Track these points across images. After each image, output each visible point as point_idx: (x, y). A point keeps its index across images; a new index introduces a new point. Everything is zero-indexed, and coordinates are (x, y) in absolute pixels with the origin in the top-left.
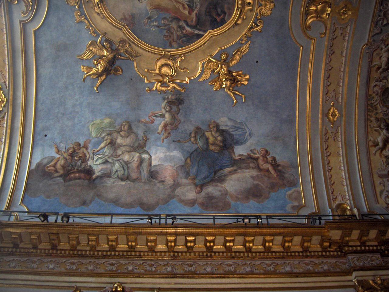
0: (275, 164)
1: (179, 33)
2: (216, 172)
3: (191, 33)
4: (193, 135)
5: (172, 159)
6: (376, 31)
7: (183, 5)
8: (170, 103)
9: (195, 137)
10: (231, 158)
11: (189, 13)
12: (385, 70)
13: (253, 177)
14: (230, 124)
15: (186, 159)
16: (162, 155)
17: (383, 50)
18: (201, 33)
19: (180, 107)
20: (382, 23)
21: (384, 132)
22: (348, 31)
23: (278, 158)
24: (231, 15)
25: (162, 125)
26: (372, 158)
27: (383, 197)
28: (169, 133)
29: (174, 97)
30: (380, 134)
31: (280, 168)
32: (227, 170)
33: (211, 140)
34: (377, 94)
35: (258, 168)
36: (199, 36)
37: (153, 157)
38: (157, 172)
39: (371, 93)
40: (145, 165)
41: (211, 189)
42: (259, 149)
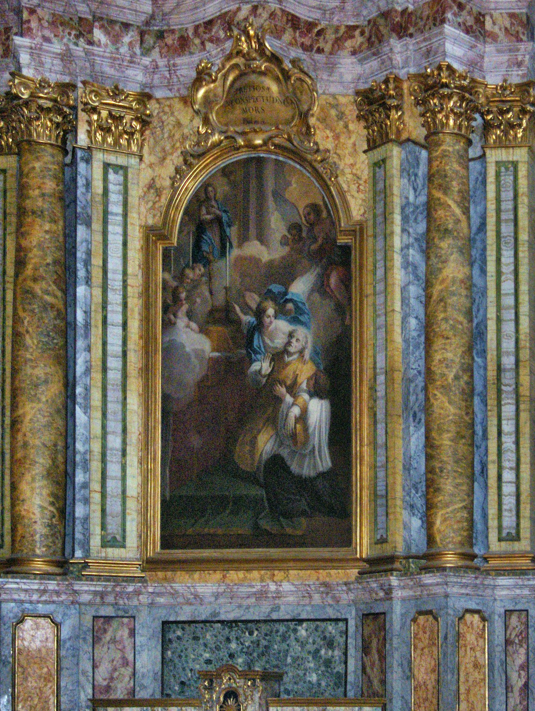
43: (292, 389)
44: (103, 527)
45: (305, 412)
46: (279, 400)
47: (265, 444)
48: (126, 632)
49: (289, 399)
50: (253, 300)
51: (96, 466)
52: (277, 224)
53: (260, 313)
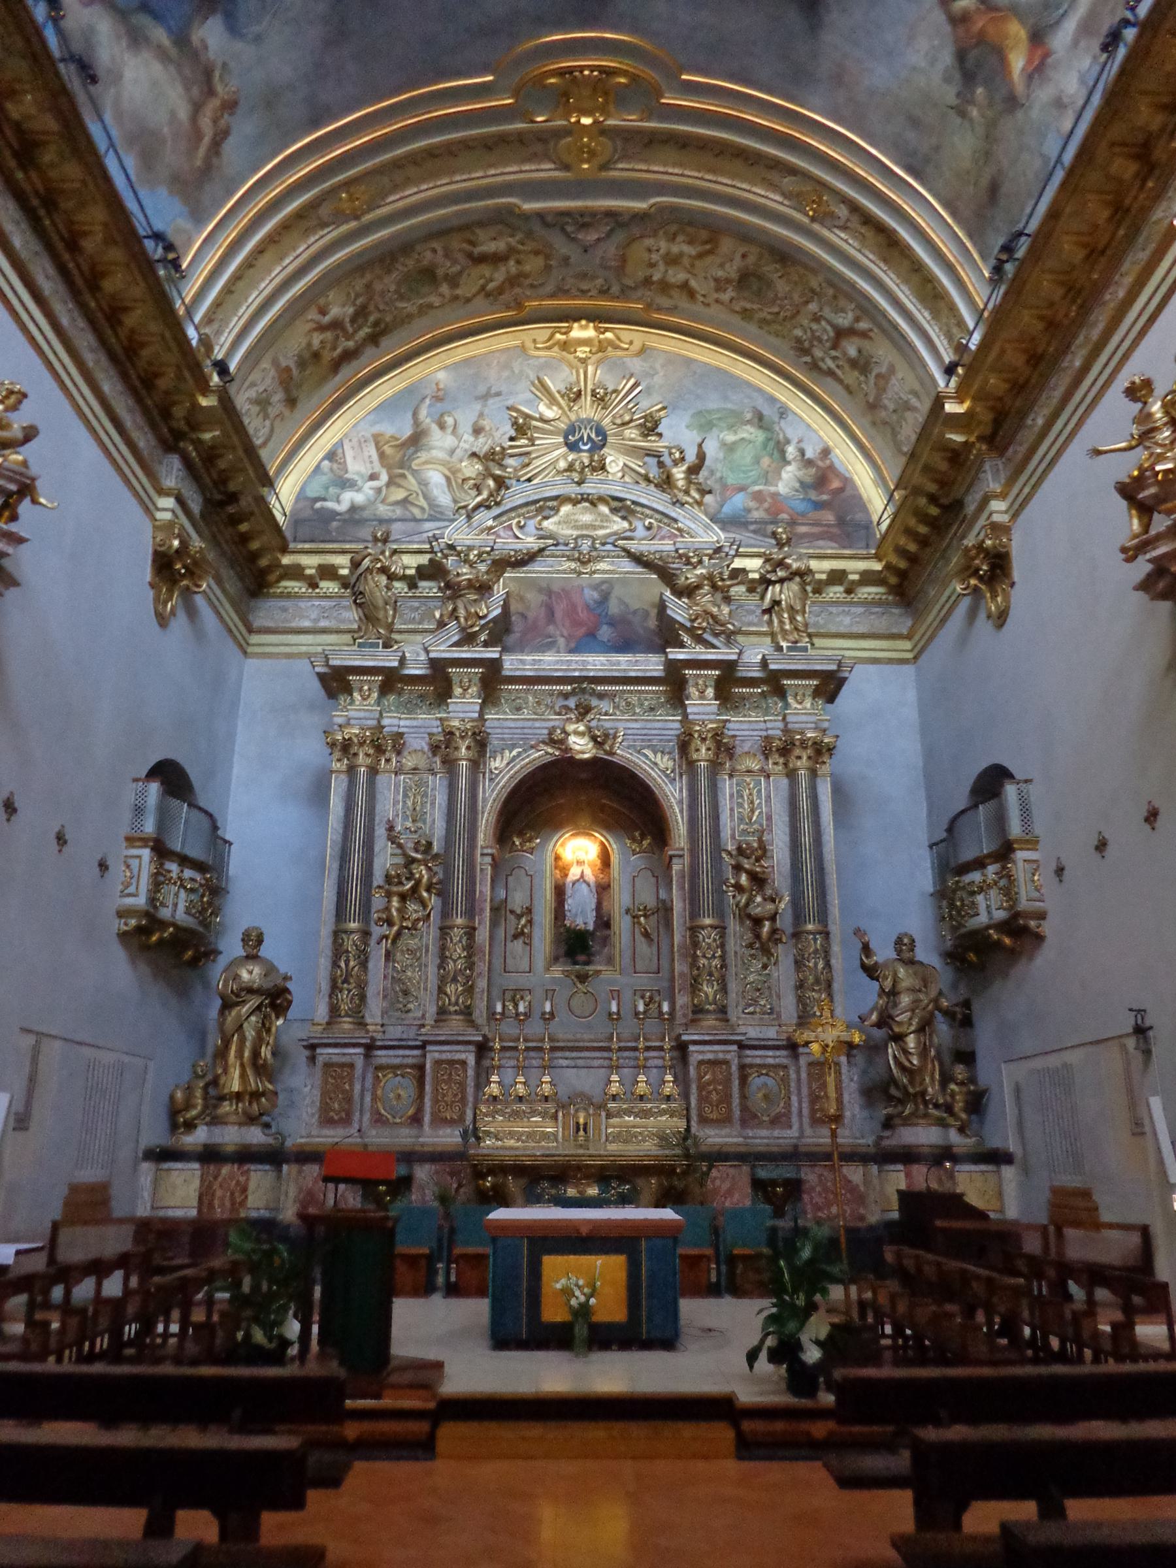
6: (549, 219)
12: (470, 256)
13: (173, 114)
17: (510, 239)
20: (567, 223)
21: (351, 310)
22: (543, 166)
26: (297, 322)
27: (247, 395)
30: (344, 306)
31: (215, 161)
32: (160, 35)
34: (418, 261)
35: (197, 108)
39: (418, 248)
42: (234, 84)
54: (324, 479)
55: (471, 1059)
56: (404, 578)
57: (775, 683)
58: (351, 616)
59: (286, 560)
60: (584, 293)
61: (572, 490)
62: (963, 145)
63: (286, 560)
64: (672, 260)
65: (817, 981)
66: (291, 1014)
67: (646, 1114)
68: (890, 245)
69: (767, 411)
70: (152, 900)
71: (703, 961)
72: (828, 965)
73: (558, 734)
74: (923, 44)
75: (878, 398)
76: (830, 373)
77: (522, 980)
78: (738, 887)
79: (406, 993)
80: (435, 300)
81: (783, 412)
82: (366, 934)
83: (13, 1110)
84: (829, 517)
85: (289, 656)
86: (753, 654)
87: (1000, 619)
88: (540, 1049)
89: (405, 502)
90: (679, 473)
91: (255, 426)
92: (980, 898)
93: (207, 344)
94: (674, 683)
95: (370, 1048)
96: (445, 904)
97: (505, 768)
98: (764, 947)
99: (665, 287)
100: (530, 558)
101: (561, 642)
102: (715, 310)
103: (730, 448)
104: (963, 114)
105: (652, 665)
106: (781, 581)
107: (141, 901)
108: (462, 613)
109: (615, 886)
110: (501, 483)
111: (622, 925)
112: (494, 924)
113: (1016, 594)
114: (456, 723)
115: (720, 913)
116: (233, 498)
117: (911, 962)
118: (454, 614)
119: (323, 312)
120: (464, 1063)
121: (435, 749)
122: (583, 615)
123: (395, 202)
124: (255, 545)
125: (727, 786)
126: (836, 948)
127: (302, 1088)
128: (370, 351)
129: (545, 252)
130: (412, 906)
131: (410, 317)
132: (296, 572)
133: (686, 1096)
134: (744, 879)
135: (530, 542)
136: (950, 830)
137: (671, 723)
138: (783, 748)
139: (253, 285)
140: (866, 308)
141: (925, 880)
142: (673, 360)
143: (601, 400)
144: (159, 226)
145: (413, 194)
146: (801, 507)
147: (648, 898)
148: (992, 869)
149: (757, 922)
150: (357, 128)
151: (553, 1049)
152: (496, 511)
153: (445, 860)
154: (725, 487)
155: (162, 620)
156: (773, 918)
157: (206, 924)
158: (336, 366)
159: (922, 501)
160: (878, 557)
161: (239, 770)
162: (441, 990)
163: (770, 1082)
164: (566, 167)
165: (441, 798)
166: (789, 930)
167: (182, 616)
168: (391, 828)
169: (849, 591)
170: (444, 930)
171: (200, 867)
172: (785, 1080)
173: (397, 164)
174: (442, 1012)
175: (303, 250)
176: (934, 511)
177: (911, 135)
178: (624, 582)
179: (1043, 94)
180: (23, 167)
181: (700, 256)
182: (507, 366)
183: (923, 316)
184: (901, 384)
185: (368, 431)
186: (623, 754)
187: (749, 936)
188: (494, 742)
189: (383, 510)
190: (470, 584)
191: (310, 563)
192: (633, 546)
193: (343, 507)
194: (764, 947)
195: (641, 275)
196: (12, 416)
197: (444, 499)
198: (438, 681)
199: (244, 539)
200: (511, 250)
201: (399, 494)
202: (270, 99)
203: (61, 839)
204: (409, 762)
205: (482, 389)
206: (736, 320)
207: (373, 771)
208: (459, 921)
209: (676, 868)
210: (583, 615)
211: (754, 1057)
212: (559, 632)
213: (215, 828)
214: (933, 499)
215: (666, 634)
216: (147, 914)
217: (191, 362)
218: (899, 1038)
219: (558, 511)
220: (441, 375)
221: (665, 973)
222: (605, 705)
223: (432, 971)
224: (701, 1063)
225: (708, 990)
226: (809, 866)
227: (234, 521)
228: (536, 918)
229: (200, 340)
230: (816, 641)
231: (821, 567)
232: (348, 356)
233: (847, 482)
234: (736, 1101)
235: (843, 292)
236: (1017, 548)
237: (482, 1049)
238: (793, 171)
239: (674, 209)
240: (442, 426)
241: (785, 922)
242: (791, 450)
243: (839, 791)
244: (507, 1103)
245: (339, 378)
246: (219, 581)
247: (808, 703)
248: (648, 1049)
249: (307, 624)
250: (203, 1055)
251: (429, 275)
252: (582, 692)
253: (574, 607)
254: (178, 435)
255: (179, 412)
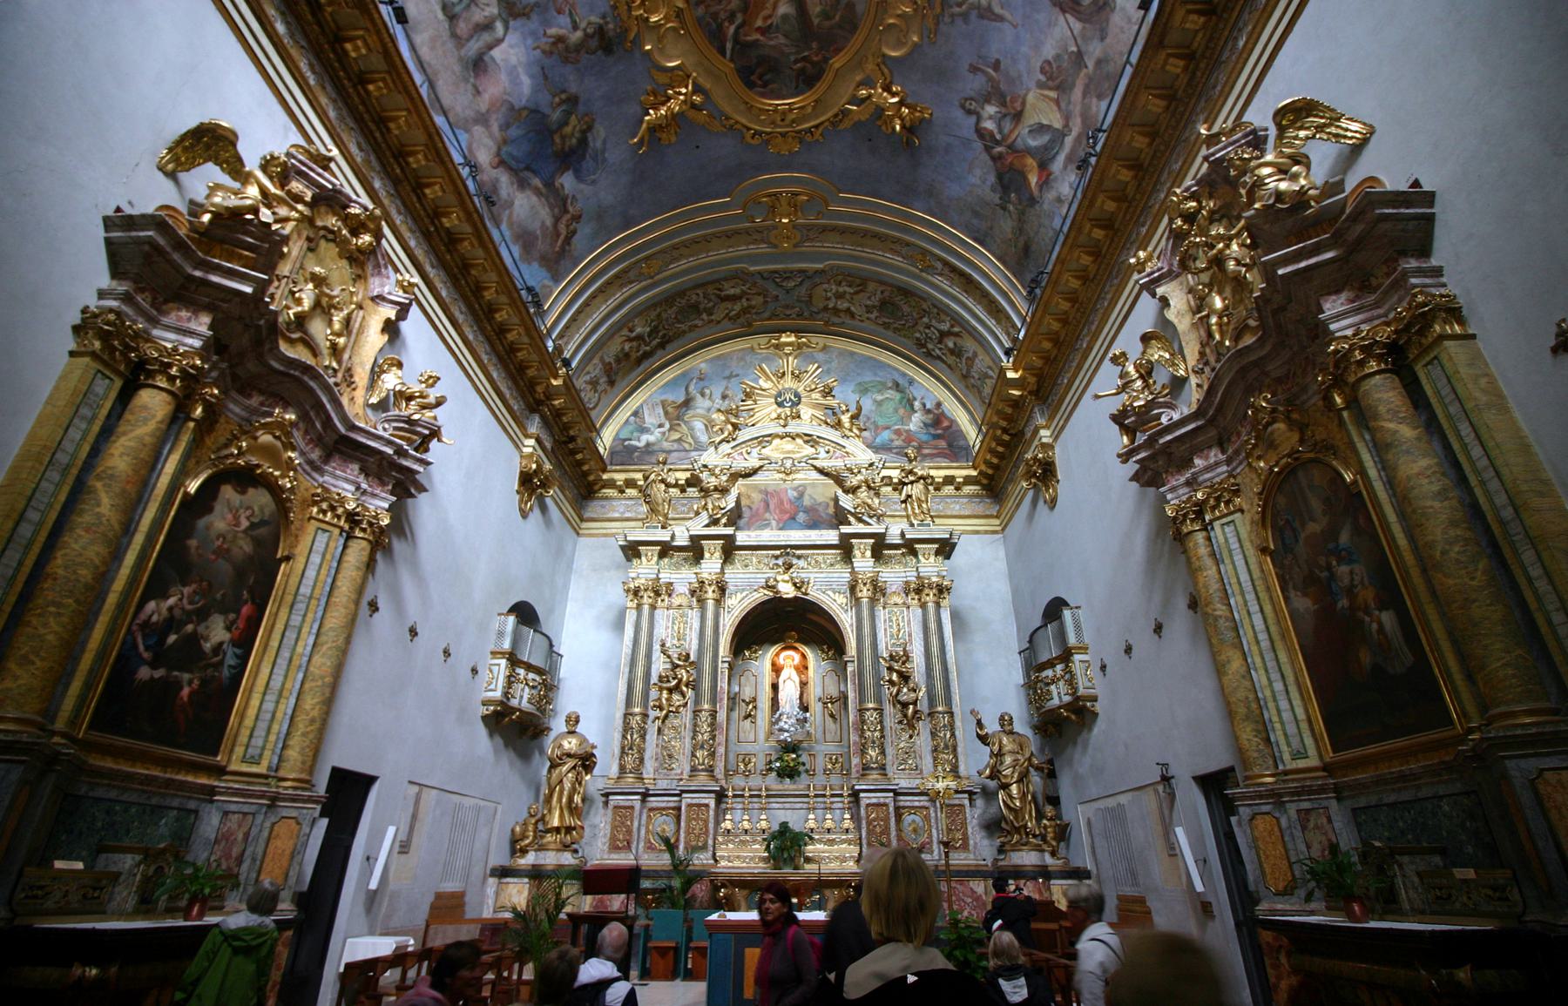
0: (568, 240)
1: (723, 15)
2: (528, 168)
3: (725, 36)
4: (563, 96)
5: (515, 80)
7: (770, 16)
8: (600, 30)
9: (562, 102)
10: (553, 177)
11: (759, 29)
12: (719, 296)
14: (599, 144)
15: (525, 108)
16: (514, 60)
18: (728, 53)
19: (599, 52)
23: (576, 237)
24: (764, 95)
25: (562, 32)
28: (551, 53)
29: (611, 34)
32: (537, 182)
33: (568, 130)
35: (557, 220)
36: (722, 52)
37: (504, 45)
38: (485, 71)
40: (486, 37)
41: (504, 180)
42: (579, 205)
43: (1367, 612)
44: (1289, 745)
45: (1380, 624)
46: (1363, 621)
47: (1365, 658)
48: (1325, 820)
49: (1367, 619)
50: (1322, 561)
51: (1271, 705)
52: (1316, 505)
53: (1329, 567)
54: (631, 428)
55: (712, 803)
56: (676, 485)
57: (910, 547)
58: (645, 508)
59: (605, 477)
60: (788, 317)
61: (780, 430)
62: (1006, 225)
63: (605, 477)
64: (839, 296)
65: (946, 747)
66: (596, 771)
67: (831, 842)
68: (969, 284)
69: (901, 381)
70: (506, 694)
71: (868, 734)
72: (953, 735)
73: (771, 583)
74: (978, 172)
75: (968, 371)
76: (939, 358)
77: (749, 748)
78: (891, 682)
79: (670, 756)
80: (700, 323)
81: (911, 382)
82: (645, 716)
83: (399, 838)
84: (943, 444)
85: (605, 535)
86: (895, 530)
87: (1052, 503)
88: (759, 796)
89: (680, 440)
90: (845, 419)
91: (588, 396)
92: (1053, 687)
93: (559, 349)
94: (845, 548)
95: (645, 795)
96: (697, 695)
97: (738, 605)
98: (910, 723)
99: (836, 311)
100: (755, 471)
101: (774, 523)
102: (866, 324)
103: (879, 404)
104: (1004, 208)
105: (831, 536)
106: (912, 483)
107: (498, 694)
108: (710, 506)
109: (811, 683)
110: (736, 427)
111: (816, 708)
112: (731, 709)
113: (1059, 487)
114: (705, 575)
115: (879, 700)
116: (572, 439)
117: (1011, 733)
118: (705, 507)
119: (631, 331)
120: (707, 806)
121: (693, 593)
122: (787, 506)
123: (675, 268)
124: (585, 468)
125: (881, 614)
126: (958, 723)
127: (599, 823)
128: (660, 352)
129: (764, 293)
130: (676, 697)
131: (684, 332)
132: (611, 484)
133: (859, 829)
134: (895, 677)
135: (753, 462)
136: (1030, 641)
137: (842, 575)
138: (917, 589)
139: (589, 316)
140: (957, 320)
141: (1018, 677)
142: (842, 353)
143: (797, 377)
144: (531, 283)
145: (683, 264)
146: (924, 438)
147: (833, 691)
148: (1059, 668)
149: (905, 705)
150: (651, 229)
151: (768, 796)
152: (733, 444)
153: (696, 665)
154: (877, 427)
155: (524, 515)
156: (915, 703)
157: (543, 711)
158: (639, 361)
159: (999, 432)
160: (975, 468)
161: (571, 608)
162: (693, 755)
163: (917, 819)
164: (775, 246)
165: (696, 625)
166: (927, 711)
167: (537, 511)
168: (663, 645)
169: (957, 489)
170: (696, 713)
171: (539, 671)
172: (927, 818)
173: (675, 247)
174: (694, 769)
175: (619, 297)
176: (1006, 437)
177: (975, 221)
178: (813, 485)
179: (1050, 196)
180: (449, 251)
181: (856, 293)
182: (742, 359)
183: (991, 323)
184: (983, 361)
185: (658, 399)
186: (814, 594)
187: (899, 715)
188: (731, 588)
189: (666, 445)
190: (716, 489)
191: (620, 478)
192: (818, 463)
193: (642, 444)
194: (910, 723)
195: (821, 305)
196: (430, 391)
197: (704, 438)
198: (695, 550)
199: (580, 463)
200: (744, 293)
201: (676, 436)
202: (600, 215)
203: (447, 653)
204: (676, 601)
205: (727, 373)
206: (881, 330)
207: (653, 607)
208: (706, 707)
209: (850, 669)
210: (787, 506)
211: (905, 801)
212: (772, 518)
213: (551, 646)
214: (1005, 431)
215: (840, 517)
216: (501, 703)
217: (552, 361)
218: (1005, 787)
219: (770, 442)
220: (703, 366)
221: (845, 742)
222: (802, 563)
223: (688, 740)
224: (868, 805)
225: (872, 753)
226: (937, 667)
227: (573, 452)
228: (759, 705)
229: (555, 348)
230: (937, 521)
231: (938, 475)
232: (647, 355)
233: (953, 422)
234: (893, 833)
235: (942, 311)
236: (1059, 456)
237: (720, 796)
238: (908, 244)
239: (839, 267)
240: (703, 395)
241: (923, 706)
242: (917, 404)
243: (955, 616)
244: (737, 836)
245: (642, 368)
246: (562, 488)
247: (932, 558)
248: (833, 796)
249: (617, 515)
250: (537, 800)
251: (695, 309)
252: (787, 552)
253: (782, 502)
254: (539, 403)
255: (539, 389)
